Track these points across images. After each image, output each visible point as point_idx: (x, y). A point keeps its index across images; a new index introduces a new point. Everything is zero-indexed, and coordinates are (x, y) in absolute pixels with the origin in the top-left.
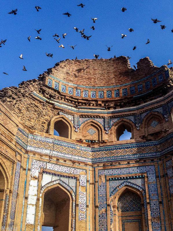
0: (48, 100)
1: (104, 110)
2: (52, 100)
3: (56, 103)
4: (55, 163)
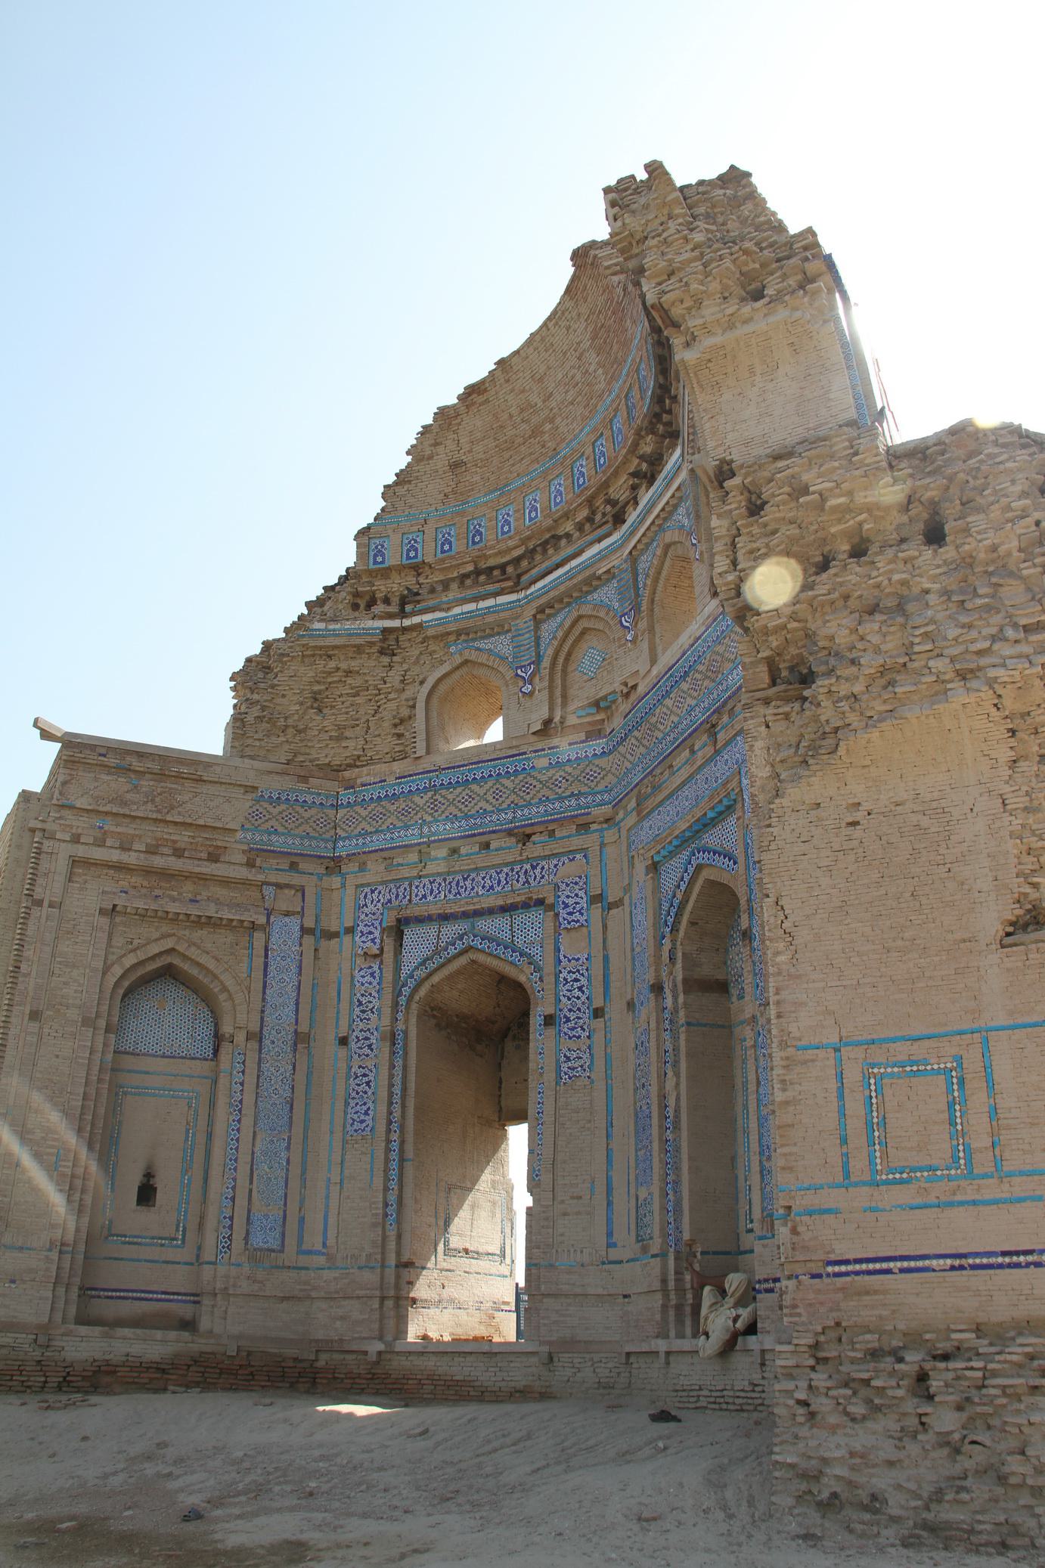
0: (395, 623)
1: (608, 535)
2: (414, 614)
3: (426, 617)
4: (442, 869)
